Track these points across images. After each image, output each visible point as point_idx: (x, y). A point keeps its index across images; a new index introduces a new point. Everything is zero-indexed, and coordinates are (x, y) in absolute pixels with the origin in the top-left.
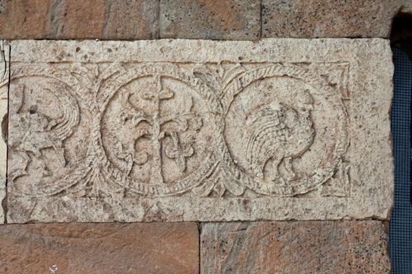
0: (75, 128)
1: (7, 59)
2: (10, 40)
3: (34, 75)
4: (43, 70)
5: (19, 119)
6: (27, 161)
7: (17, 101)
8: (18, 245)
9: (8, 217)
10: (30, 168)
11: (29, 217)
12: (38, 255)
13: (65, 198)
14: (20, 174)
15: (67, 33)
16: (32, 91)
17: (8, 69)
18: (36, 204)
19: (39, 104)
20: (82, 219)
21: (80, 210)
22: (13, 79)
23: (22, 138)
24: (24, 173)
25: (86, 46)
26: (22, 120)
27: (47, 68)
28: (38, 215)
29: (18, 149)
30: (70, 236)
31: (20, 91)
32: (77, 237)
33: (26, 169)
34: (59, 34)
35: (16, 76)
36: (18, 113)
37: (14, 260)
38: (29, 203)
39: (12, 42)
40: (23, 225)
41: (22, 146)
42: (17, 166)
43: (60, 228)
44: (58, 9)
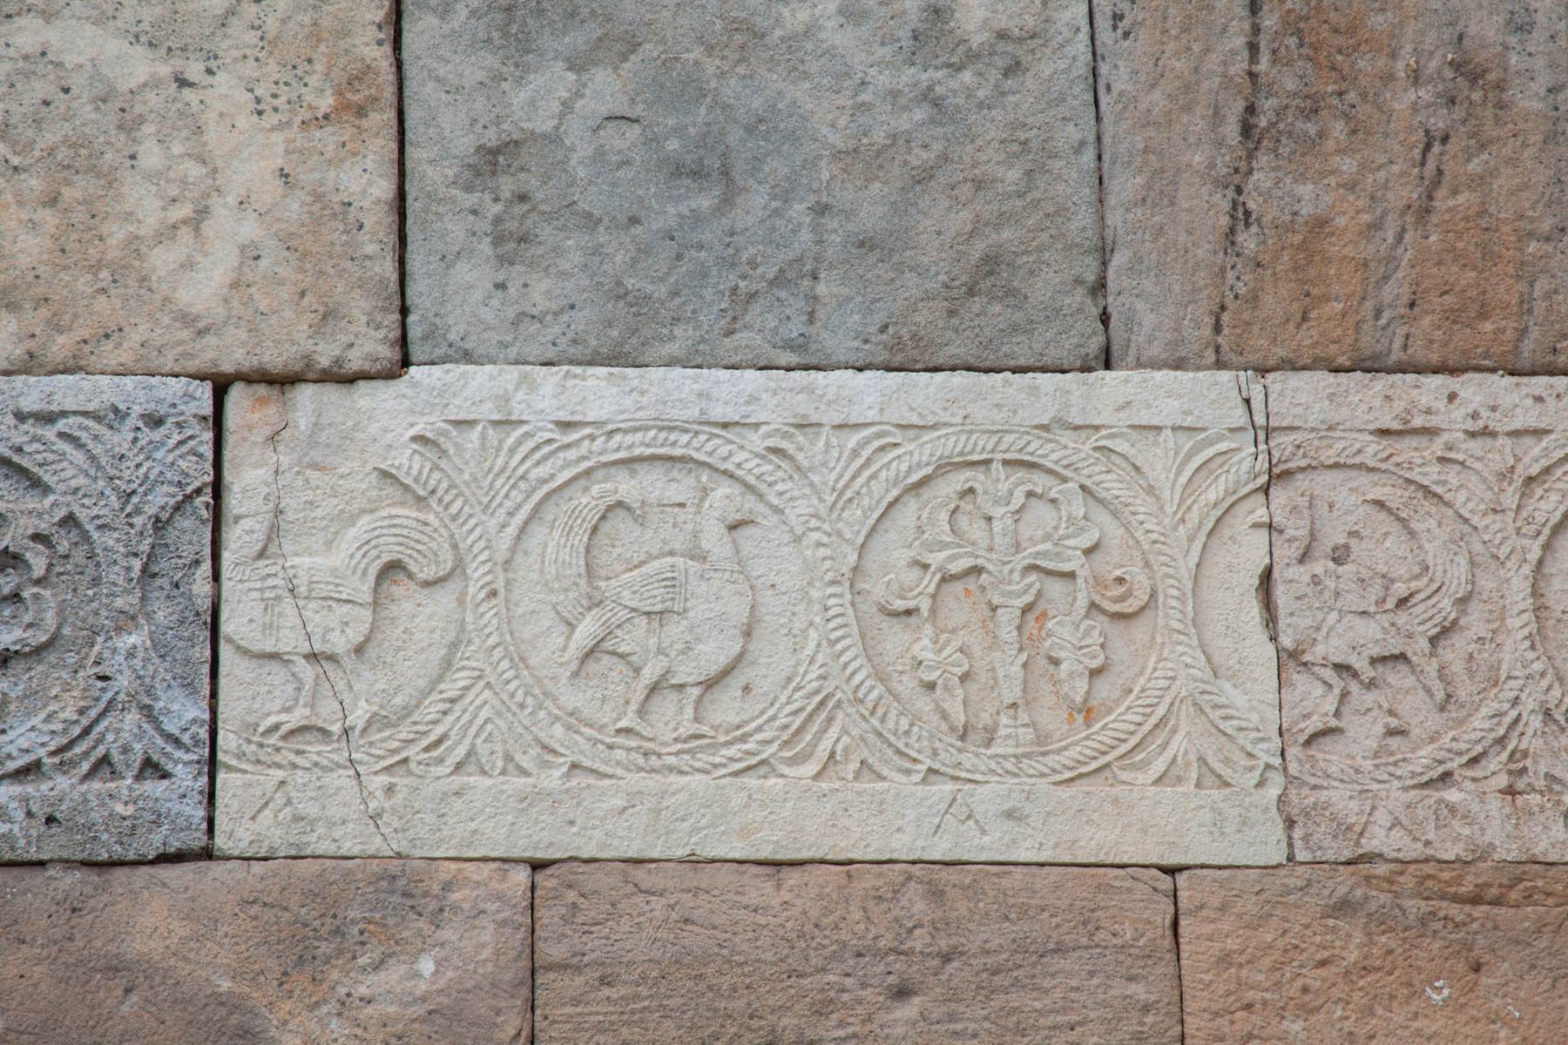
0: (1463, 602)
1: (1260, 420)
2: (1263, 371)
3: (1336, 466)
4: (1359, 451)
5: (1307, 578)
6: (1337, 691)
7: (1297, 529)
8: (1331, 922)
9: (1298, 844)
10: (1346, 710)
11: (1357, 844)
12: (1390, 952)
13: (1453, 795)
14: (1320, 726)
15: (1418, 352)
16: (1331, 506)
17: (1262, 447)
18: (1374, 808)
19: (1353, 542)
20: (1508, 851)
21: (1489, 826)
22: (1279, 476)
23: (1318, 629)
24: (1333, 723)
25: (1476, 390)
26: (1316, 580)
27: (1373, 449)
28: (1379, 839)
29: (1307, 658)
30: (1476, 900)
31: (1302, 502)
32: (1496, 902)
33: (1337, 714)
34: (1396, 355)
35: (1290, 465)
36: (1301, 561)
37: (1323, 963)
38: (1354, 805)
39: (1270, 377)
40: (1341, 868)
41: (1320, 650)
42: (1308, 705)
43: (1446, 875)
44: (1389, 292)
